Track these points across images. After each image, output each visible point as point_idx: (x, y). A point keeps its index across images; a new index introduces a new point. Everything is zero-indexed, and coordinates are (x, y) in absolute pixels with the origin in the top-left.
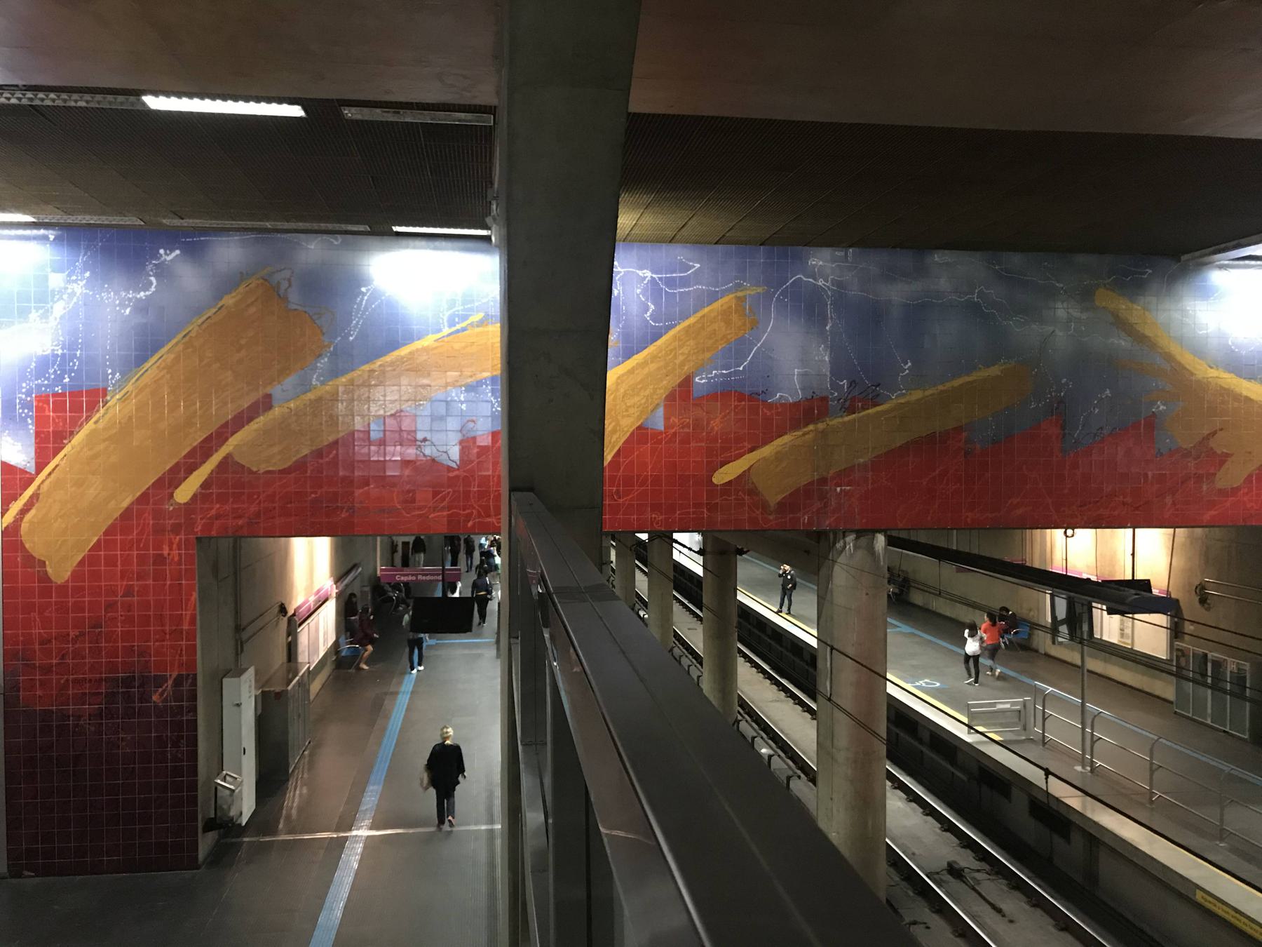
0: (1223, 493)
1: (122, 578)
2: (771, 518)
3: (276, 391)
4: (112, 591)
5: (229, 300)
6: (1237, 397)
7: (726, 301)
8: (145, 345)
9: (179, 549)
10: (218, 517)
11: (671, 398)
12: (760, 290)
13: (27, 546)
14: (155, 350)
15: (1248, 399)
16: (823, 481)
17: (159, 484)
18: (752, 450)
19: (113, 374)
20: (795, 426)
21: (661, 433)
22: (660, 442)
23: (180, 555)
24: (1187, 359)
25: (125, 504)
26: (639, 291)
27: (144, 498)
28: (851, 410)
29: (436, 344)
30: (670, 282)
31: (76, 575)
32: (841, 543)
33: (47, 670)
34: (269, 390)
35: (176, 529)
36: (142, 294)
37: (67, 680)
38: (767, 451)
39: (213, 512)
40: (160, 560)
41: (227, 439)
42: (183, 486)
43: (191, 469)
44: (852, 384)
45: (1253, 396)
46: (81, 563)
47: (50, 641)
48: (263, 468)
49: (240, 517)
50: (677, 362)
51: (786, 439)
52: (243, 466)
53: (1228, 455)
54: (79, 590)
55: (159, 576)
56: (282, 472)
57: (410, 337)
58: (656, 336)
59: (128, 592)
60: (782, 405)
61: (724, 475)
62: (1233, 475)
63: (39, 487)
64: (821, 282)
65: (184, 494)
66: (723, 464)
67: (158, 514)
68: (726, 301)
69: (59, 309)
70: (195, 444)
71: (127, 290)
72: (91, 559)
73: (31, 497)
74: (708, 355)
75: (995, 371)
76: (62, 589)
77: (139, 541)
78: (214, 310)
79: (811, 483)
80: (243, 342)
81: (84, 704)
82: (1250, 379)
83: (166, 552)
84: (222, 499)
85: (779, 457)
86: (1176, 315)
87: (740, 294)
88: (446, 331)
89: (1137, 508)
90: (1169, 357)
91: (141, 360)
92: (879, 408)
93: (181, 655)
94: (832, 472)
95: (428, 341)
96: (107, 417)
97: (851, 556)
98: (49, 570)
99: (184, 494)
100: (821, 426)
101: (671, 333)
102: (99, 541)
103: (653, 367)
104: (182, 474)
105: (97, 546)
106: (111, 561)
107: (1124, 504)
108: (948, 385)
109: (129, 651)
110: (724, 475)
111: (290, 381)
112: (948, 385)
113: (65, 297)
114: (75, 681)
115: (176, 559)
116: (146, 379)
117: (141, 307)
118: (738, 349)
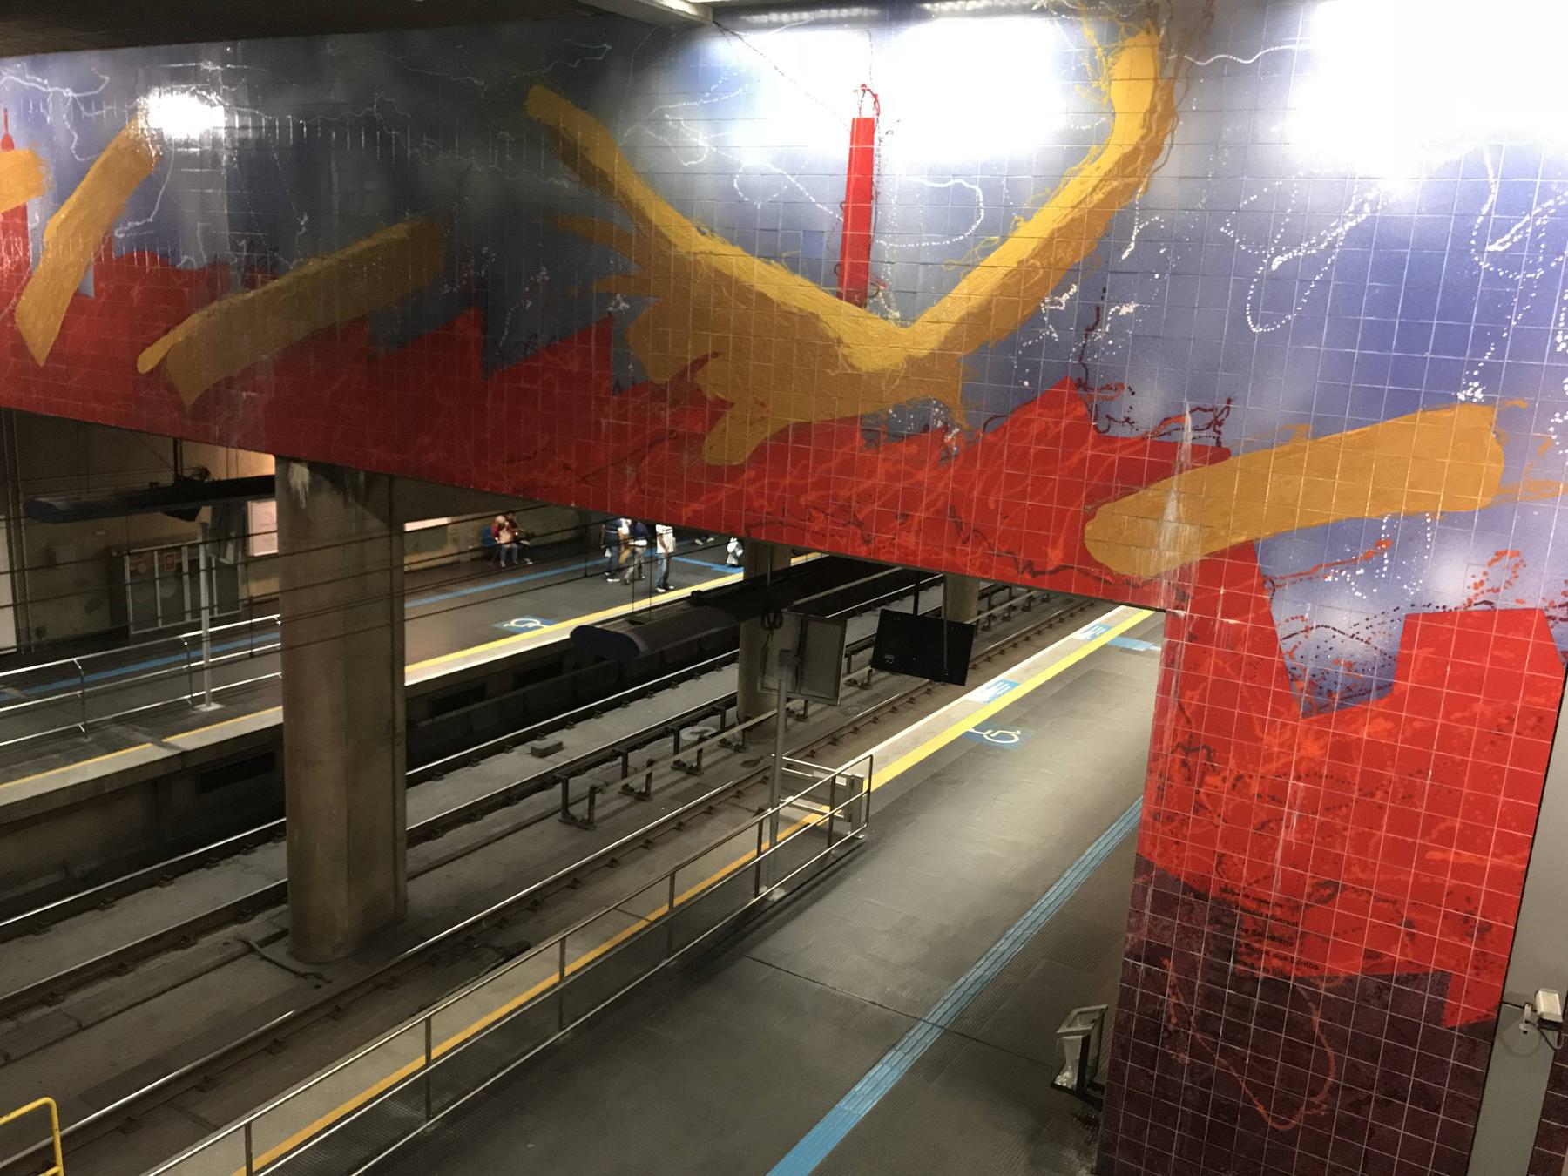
0: (715, 472)
6: (744, 292)
15: (762, 297)
16: (229, 382)
18: (166, 332)
20: (202, 304)
24: (660, 213)
28: (251, 284)
38: (178, 335)
45: (773, 293)
51: (195, 320)
53: (723, 404)
60: (190, 273)
61: (148, 360)
62: (731, 444)
75: (398, 232)
82: (769, 256)
89: (584, 479)
90: (636, 214)
107: (567, 468)
108: (348, 252)
110: (148, 360)
112: (348, 252)
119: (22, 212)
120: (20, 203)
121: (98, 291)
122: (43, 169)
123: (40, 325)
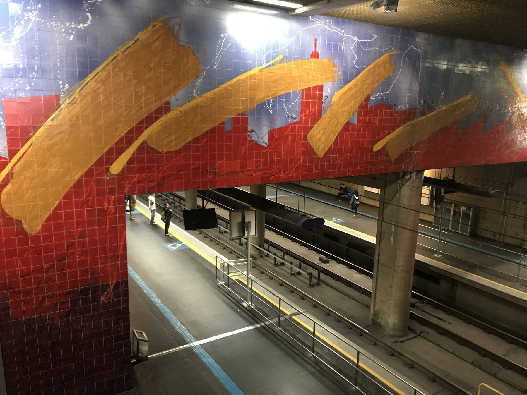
1: (77, 226)
2: (392, 167)
3: (172, 99)
4: (71, 236)
5: (141, 36)
7: (385, 56)
8: (85, 65)
9: (115, 204)
10: (139, 182)
11: (360, 107)
12: (398, 52)
13: (7, 211)
14: (93, 68)
16: (411, 149)
17: (99, 162)
18: (388, 134)
19: (63, 84)
20: (404, 123)
21: (355, 126)
22: (354, 131)
23: (115, 208)
25: (77, 177)
26: (352, 48)
27: (89, 173)
28: (423, 114)
29: (259, 73)
30: (365, 44)
31: (46, 227)
32: (409, 176)
33: (29, 293)
34: (167, 99)
35: (112, 192)
36: (81, 25)
37: (44, 297)
38: (393, 135)
39: (135, 179)
40: (102, 212)
41: (142, 132)
42: (115, 164)
43: (120, 151)
44: (424, 102)
46: (48, 219)
47: (29, 274)
48: (165, 150)
49: (152, 181)
50: (364, 88)
51: (401, 128)
52: (153, 149)
54: (47, 238)
55: (101, 223)
56: (176, 152)
57: (246, 68)
58: (357, 74)
59: (82, 235)
60: (401, 111)
61: (377, 147)
63: (12, 168)
64: (419, 51)
65: (116, 168)
66: (378, 141)
67: (100, 182)
68: (385, 56)
69: (18, 31)
70: (122, 135)
71: (70, 21)
72: (55, 216)
73: (7, 175)
74: (376, 85)
76: (36, 238)
77: (87, 201)
78: (132, 42)
79: (407, 150)
80: (152, 65)
81: (57, 310)
83: (106, 207)
84: (141, 170)
85: (398, 136)
86: (519, 77)
87: (390, 53)
88: (265, 65)
91: (83, 75)
92: (432, 114)
93: (118, 270)
94: (414, 144)
95: (255, 71)
96: (60, 117)
97: (414, 182)
98: (25, 226)
99: (116, 168)
100: (413, 122)
101: (363, 72)
102: (60, 203)
103: (354, 90)
104: (115, 156)
105: (58, 208)
106: (69, 216)
109: (84, 273)
110: (377, 147)
111: (180, 94)
113: (22, 22)
114: (48, 297)
115: (113, 211)
116: (88, 89)
117: (81, 36)
118: (387, 83)
119: (321, 88)
120: (319, 83)
121: (359, 121)
122: (336, 69)
123: (323, 139)
